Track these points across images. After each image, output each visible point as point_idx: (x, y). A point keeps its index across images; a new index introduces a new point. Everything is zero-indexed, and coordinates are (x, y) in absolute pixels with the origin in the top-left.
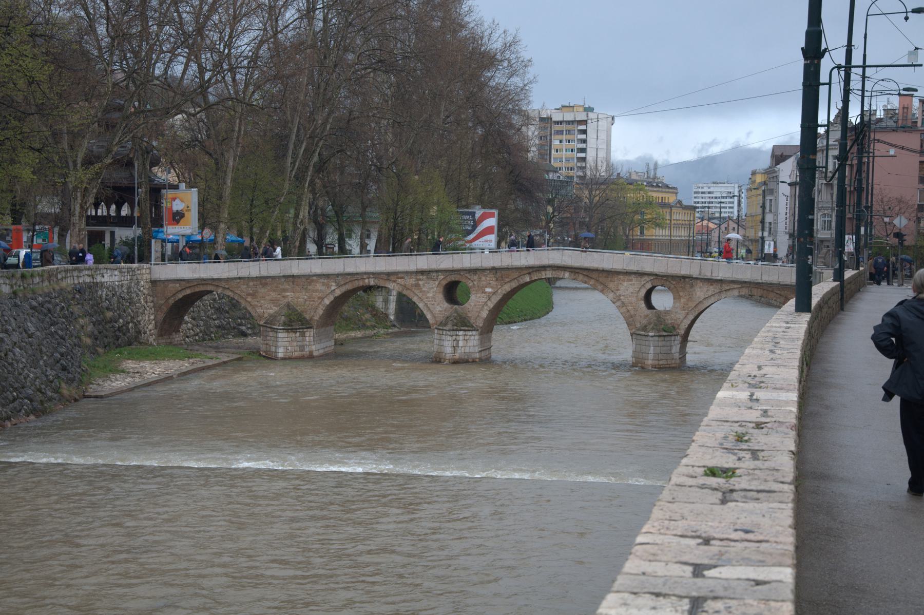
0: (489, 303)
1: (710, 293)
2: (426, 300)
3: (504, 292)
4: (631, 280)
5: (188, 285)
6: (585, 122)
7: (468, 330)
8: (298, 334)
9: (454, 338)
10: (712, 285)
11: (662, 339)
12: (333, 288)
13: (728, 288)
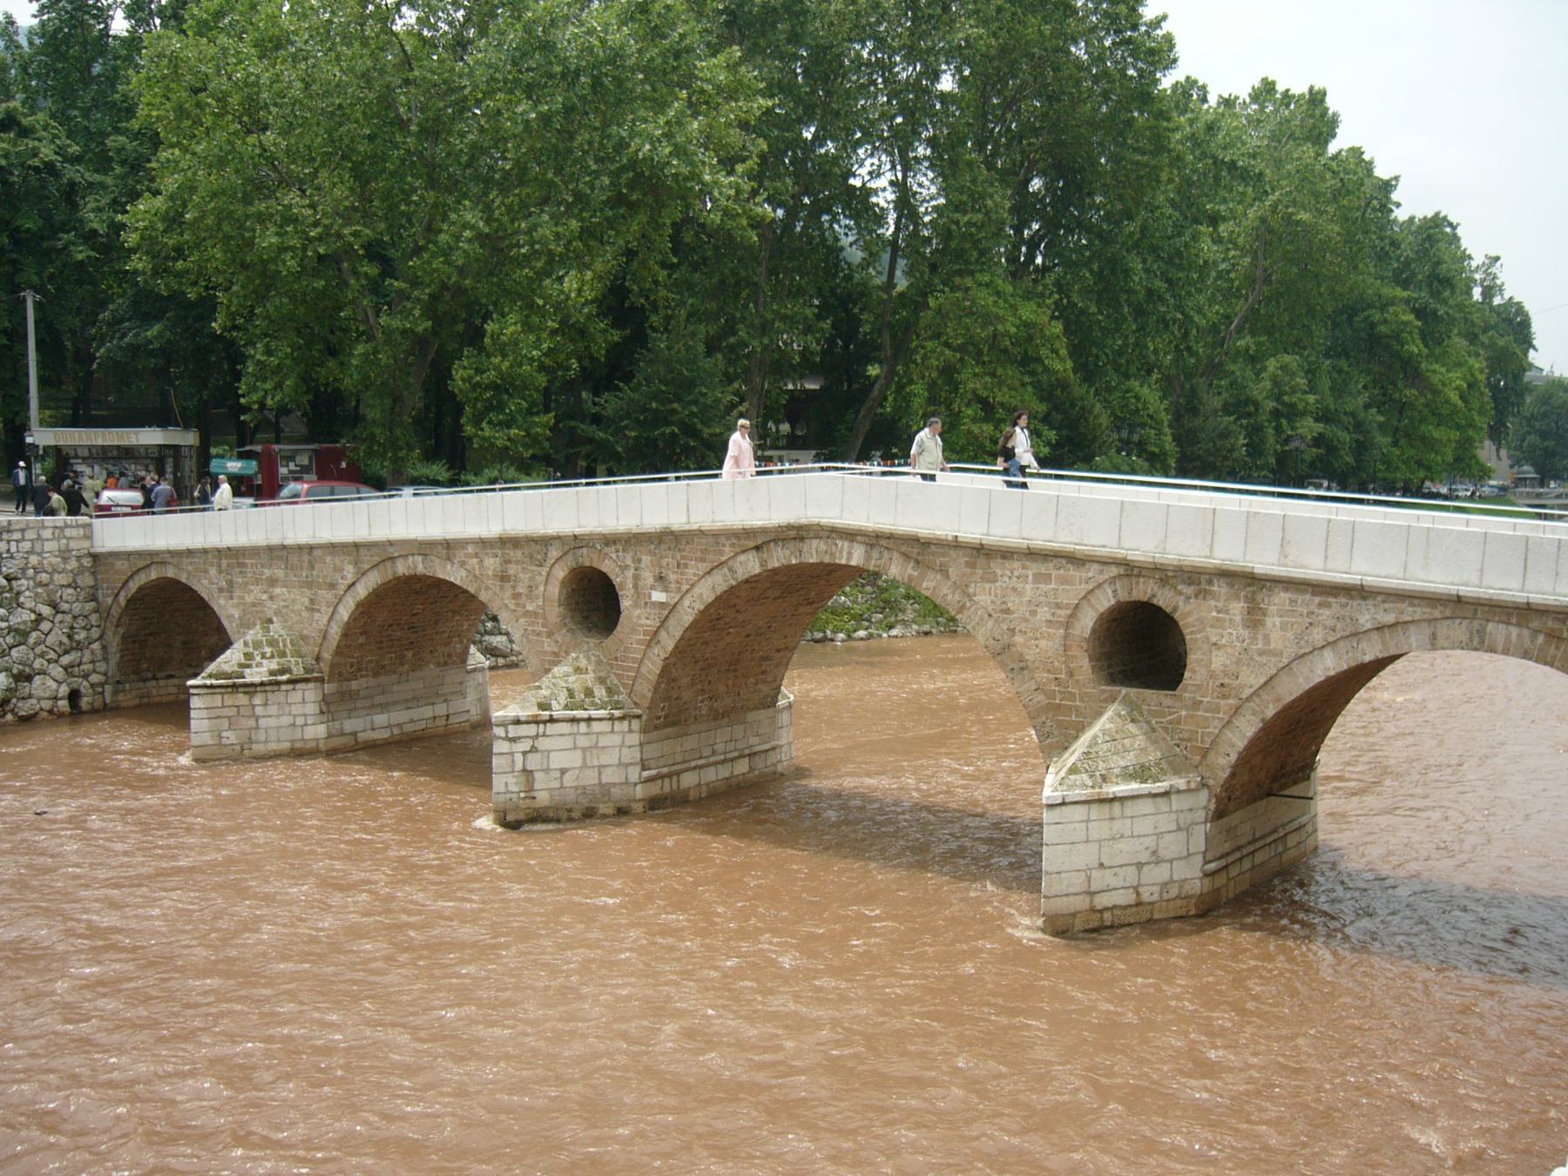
1: (1318, 636)
4: (1047, 578)
5: (141, 564)
8: (258, 700)
9: (525, 745)
12: (350, 578)
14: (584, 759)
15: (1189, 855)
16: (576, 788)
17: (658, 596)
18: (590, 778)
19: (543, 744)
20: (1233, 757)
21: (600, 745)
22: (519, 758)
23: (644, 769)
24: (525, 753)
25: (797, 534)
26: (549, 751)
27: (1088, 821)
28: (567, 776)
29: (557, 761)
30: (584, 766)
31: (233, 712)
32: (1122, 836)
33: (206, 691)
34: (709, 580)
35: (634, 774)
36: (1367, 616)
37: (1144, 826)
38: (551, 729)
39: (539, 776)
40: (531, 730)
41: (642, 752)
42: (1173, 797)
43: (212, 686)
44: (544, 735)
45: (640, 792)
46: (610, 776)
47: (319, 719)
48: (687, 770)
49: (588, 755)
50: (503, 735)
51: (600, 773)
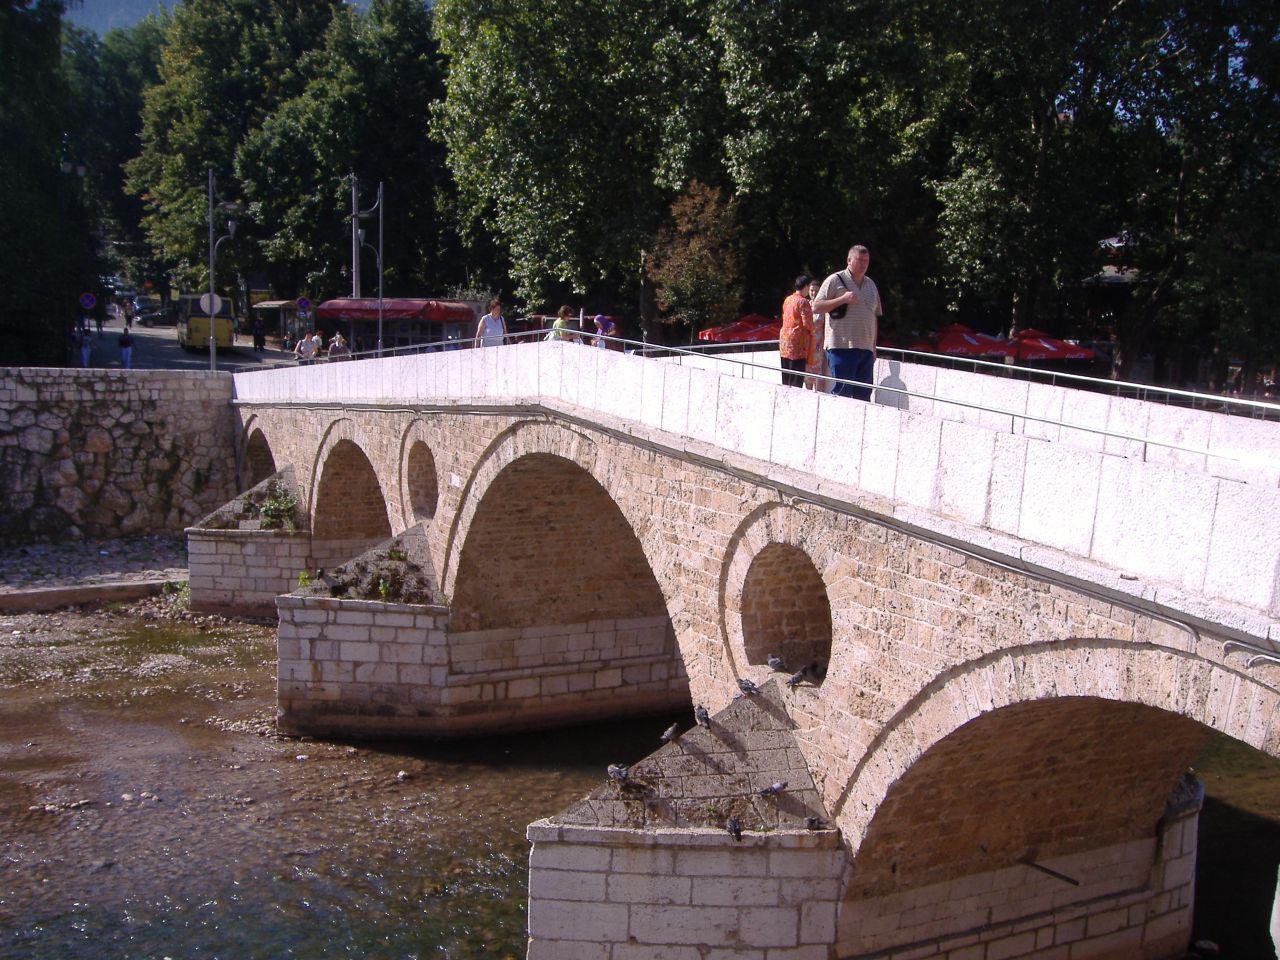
1: (974, 643)
7: (386, 611)
8: (250, 549)
9: (314, 632)
10: (981, 587)
11: (663, 860)
13: (1063, 632)
14: (381, 653)
15: (799, 944)
16: (371, 684)
18: (387, 676)
19: (330, 631)
20: (871, 813)
21: (399, 641)
22: (306, 645)
23: (452, 672)
24: (312, 641)
25: (529, 413)
26: (340, 641)
27: (609, 872)
28: (360, 672)
29: (349, 653)
30: (381, 662)
31: (227, 559)
32: (671, 903)
33: (199, 538)
35: (439, 676)
36: (1058, 617)
37: (719, 893)
38: (344, 617)
39: (329, 667)
40: (320, 616)
41: (449, 654)
42: (774, 856)
43: (205, 534)
44: (335, 623)
45: (446, 696)
46: (414, 676)
48: (521, 678)
49: (385, 650)
50: (288, 618)
51: (399, 671)
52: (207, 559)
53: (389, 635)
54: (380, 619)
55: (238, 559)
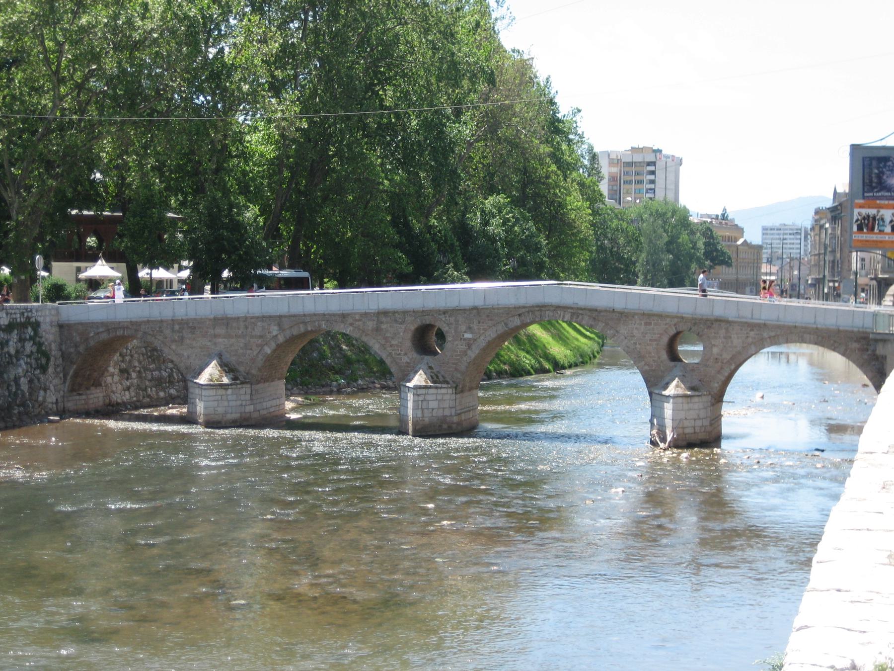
0: (469, 352)
1: (750, 340)
2: (389, 349)
3: (489, 339)
6: (653, 164)
7: (441, 388)
9: (421, 398)
12: (275, 333)
17: (468, 336)
18: (440, 413)
24: (422, 401)
34: (494, 329)
39: (426, 411)
47: (248, 403)
52: (211, 399)
53: (439, 397)
54: (439, 391)
55: (224, 398)
